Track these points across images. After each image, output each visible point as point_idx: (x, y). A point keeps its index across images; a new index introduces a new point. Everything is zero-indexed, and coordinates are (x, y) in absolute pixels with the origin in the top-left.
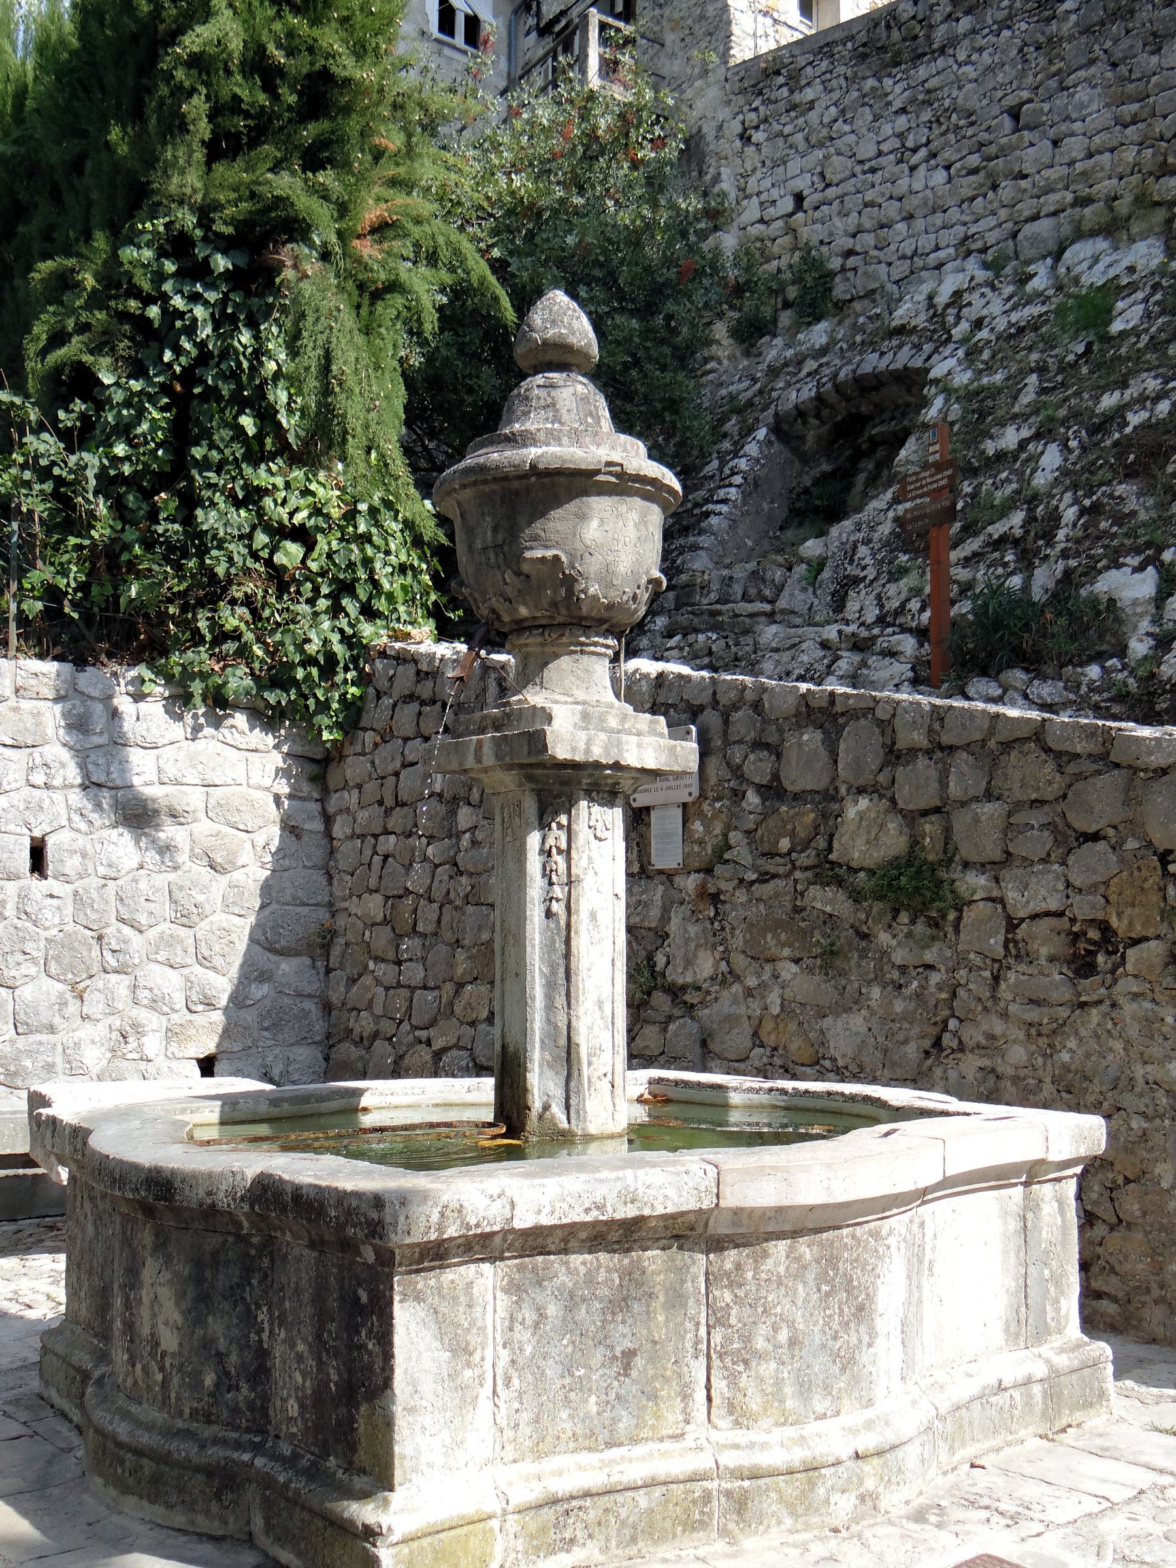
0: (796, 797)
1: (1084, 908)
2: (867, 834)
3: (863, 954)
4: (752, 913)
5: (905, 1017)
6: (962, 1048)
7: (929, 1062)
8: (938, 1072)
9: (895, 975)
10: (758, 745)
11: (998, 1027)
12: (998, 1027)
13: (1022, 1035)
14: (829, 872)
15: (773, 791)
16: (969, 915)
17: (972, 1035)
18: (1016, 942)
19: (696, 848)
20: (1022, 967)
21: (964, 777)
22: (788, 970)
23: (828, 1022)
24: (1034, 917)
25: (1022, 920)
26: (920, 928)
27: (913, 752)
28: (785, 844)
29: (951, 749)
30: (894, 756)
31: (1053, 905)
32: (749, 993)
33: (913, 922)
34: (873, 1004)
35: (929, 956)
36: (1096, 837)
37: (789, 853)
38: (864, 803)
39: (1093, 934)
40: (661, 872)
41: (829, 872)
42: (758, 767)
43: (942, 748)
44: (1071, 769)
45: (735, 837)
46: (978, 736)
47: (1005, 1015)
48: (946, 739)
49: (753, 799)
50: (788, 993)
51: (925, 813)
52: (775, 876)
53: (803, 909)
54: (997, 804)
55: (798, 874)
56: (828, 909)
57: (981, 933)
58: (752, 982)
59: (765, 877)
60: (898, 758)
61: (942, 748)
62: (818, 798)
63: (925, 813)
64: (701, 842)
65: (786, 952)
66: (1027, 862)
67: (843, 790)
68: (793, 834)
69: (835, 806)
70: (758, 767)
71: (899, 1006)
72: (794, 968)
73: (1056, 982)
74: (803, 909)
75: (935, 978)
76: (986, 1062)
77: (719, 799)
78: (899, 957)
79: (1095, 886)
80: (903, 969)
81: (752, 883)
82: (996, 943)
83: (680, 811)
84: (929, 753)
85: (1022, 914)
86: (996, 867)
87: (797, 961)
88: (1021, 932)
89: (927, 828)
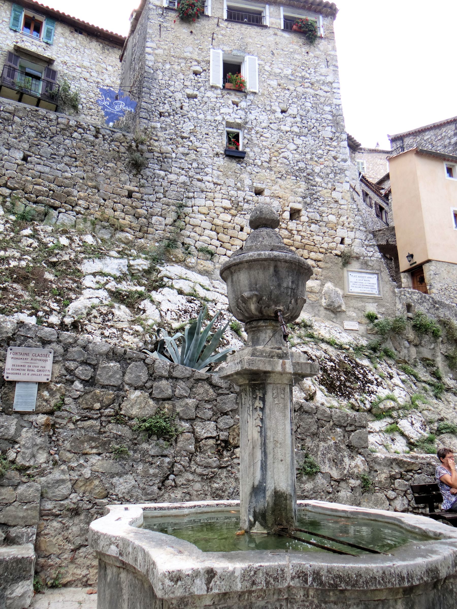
0: (103, 387)
1: (223, 435)
2: (137, 404)
3: (135, 451)
4: (77, 433)
5: (155, 475)
6: (176, 486)
7: (162, 492)
8: (166, 495)
9: (150, 459)
10: (84, 363)
11: (191, 477)
12: (191, 477)
13: (200, 479)
14: (119, 418)
15: (90, 382)
16: (181, 438)
17: (181, 480)
18: (200, 447)
19: (45, 403)
20: (202, 455)
21: (181, 388)
22: (94, 459)
23: (114, 480)
24: (206, 438)
25: (202, 440)
26: (161, 441)
27: (161, 377)
28: (97, 406)
29: (177, 379)
30: (153, 376)
31: (215, 434)
32: (72, 469)
33: (158, 439)
34: (138, 471)
35: (165, 452)
36: (226, 414)
37: (99, 409)
38: (138, 393)
39: (223, 444)
40: (17, 412)
41: (119, 418)
42: (83, 372)
43: (172, 378)
44: (220, 391)
45: (67, 400)
46: (188, 376)
47: (193, 473)
48: (175, 374)
49: (78, 385)
50: (95, 468)
51: (164, 400)
52: (90, 418)
53: (105, 432)
54: (194, 400)
55: (103, 419)
56: (119, 433)
57: (186, 443)
58: (74, 464)
59: (85, 418)
60: (155, 379)
61: (172, 378)
62: (115, 389)
63: (164, 400)
64: (46, 401)
65: (94, 451)
66: (203, 420)
67: (127, 387)
68: (101, 402)
69: (122, 393)
70: (83, 372)
71: (151, 471)
72: (98, 458)
73: (214, 461)
74: (105, 432)
75: (167, 460)
76: (186, 490)
77: (57, 383)
78: (152, 452)
79: (226, 429)
80: (153, 456)
81: (77, 421)
82: (192, 448)
83: (37, 386)
84: (167, 379)
85: (202, 437)
86: (191, 420)
87: (99, 454)
88: (201, 444)
89: (167, 406)
